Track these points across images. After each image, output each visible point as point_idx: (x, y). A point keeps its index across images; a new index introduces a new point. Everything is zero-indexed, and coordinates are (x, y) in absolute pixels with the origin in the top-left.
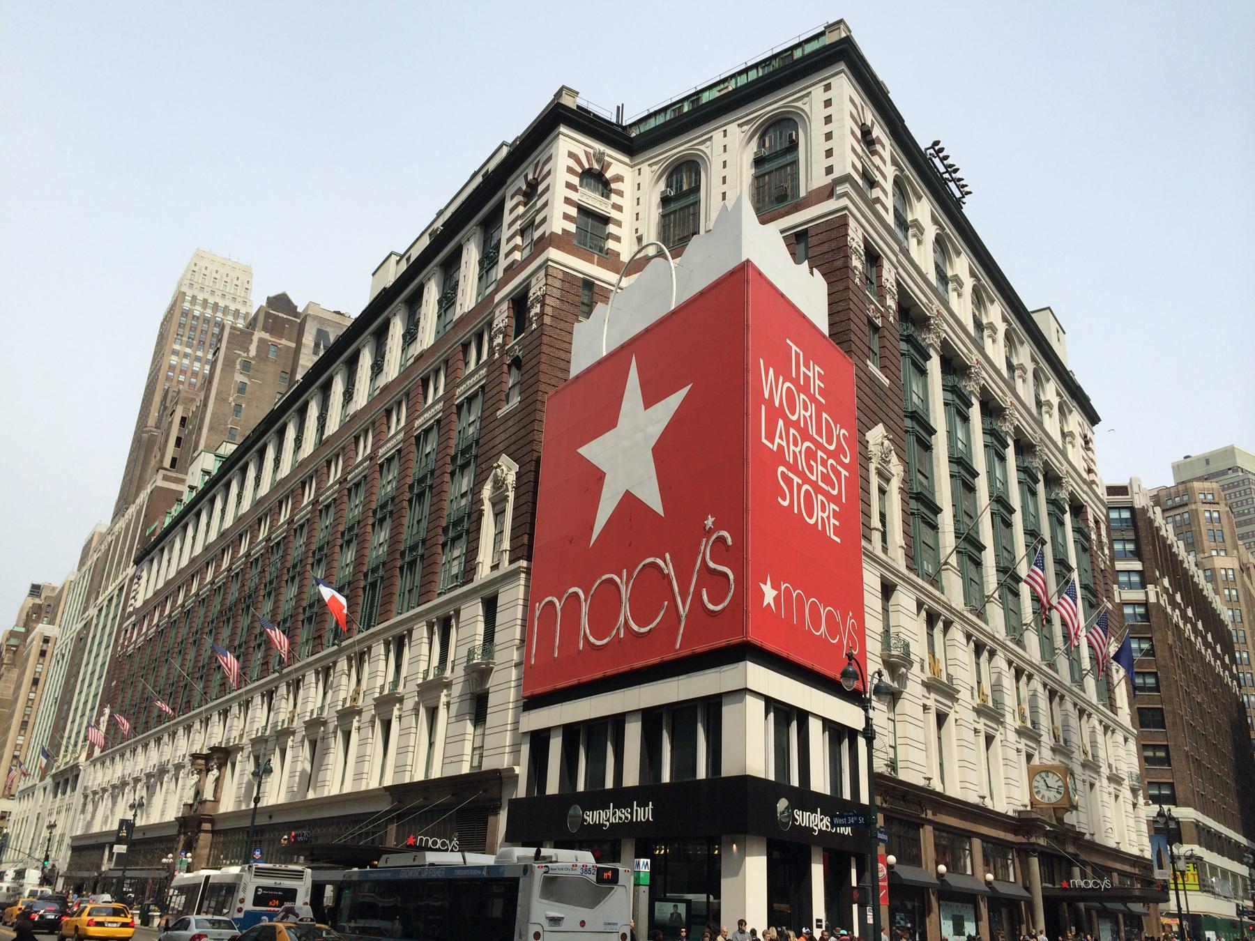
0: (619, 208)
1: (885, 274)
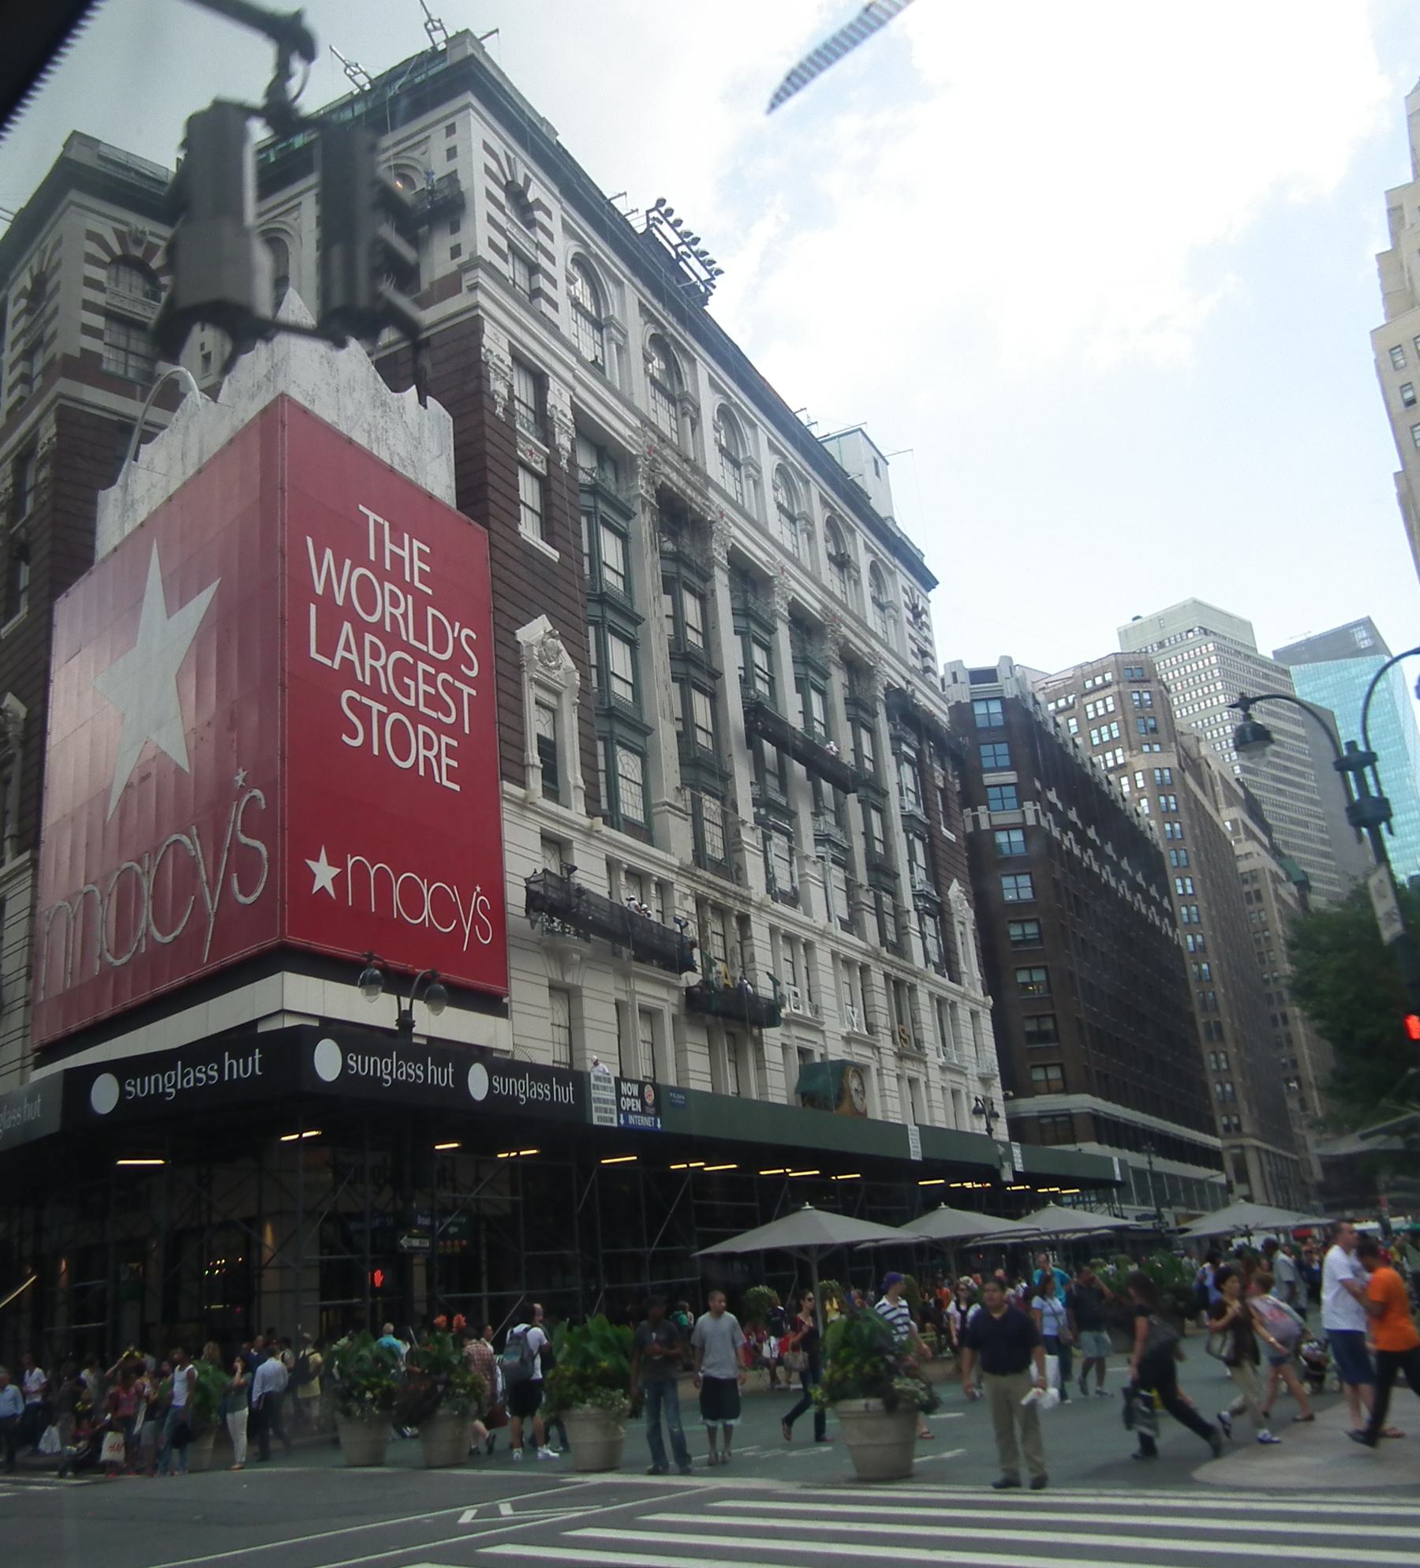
1: (551, 399)
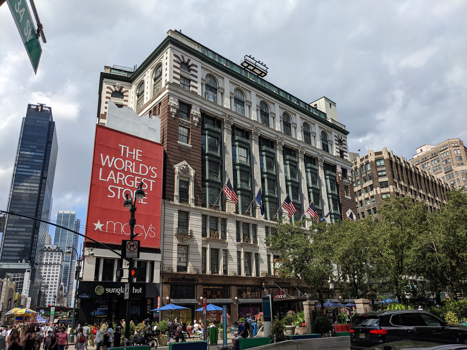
0: (127, 101)
